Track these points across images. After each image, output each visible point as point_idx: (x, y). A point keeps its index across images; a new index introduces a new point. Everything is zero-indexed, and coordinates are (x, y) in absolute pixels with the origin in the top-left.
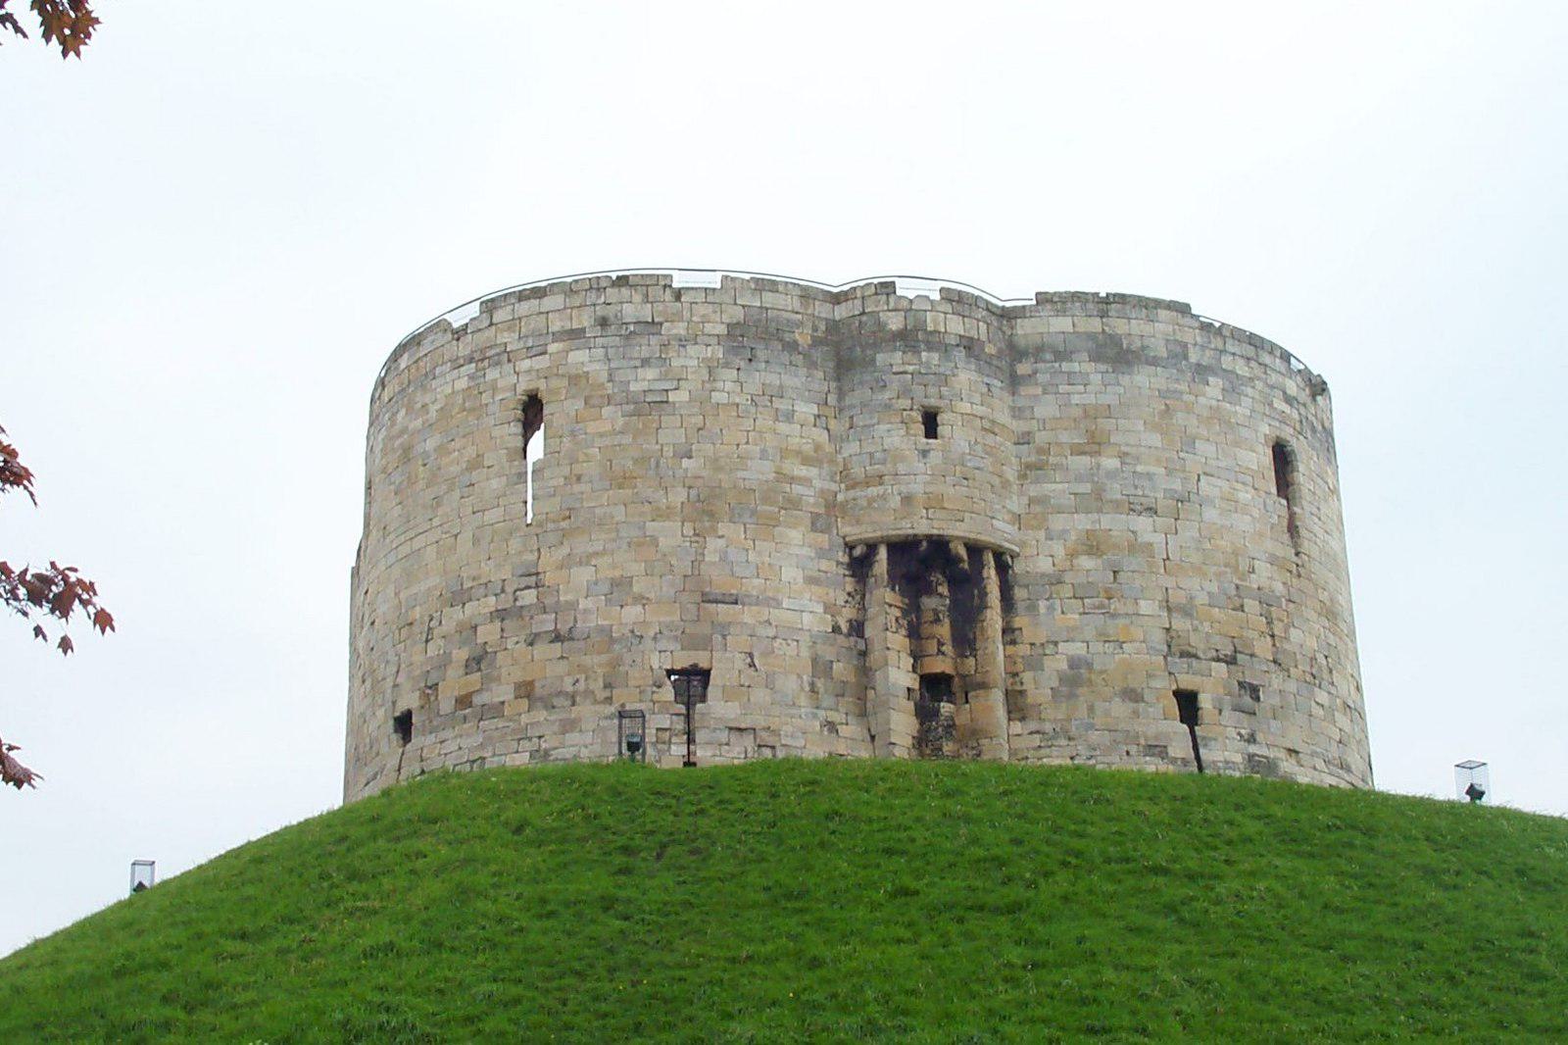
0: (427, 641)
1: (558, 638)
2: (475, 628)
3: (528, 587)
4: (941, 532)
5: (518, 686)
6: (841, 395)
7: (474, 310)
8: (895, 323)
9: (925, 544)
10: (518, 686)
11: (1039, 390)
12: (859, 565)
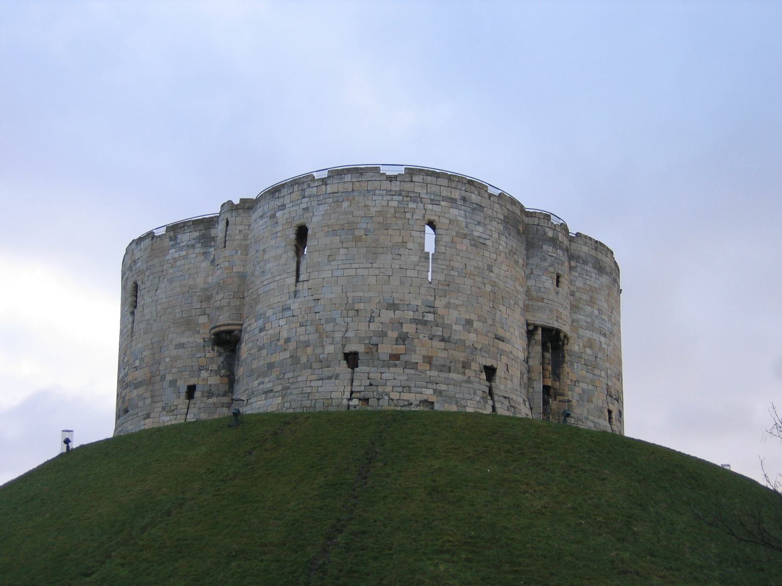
0: (369, 322)
1: (443, 340)
2: (402, 324)
3: (429, 312)
4: (560, 328)
5: (425, 357)
6: (528, 258)
7: (402, 171)
8: (550, 234)
9: (555, 331)
10: (425, 357)
11: (577, 275)
12: (530, 333)
